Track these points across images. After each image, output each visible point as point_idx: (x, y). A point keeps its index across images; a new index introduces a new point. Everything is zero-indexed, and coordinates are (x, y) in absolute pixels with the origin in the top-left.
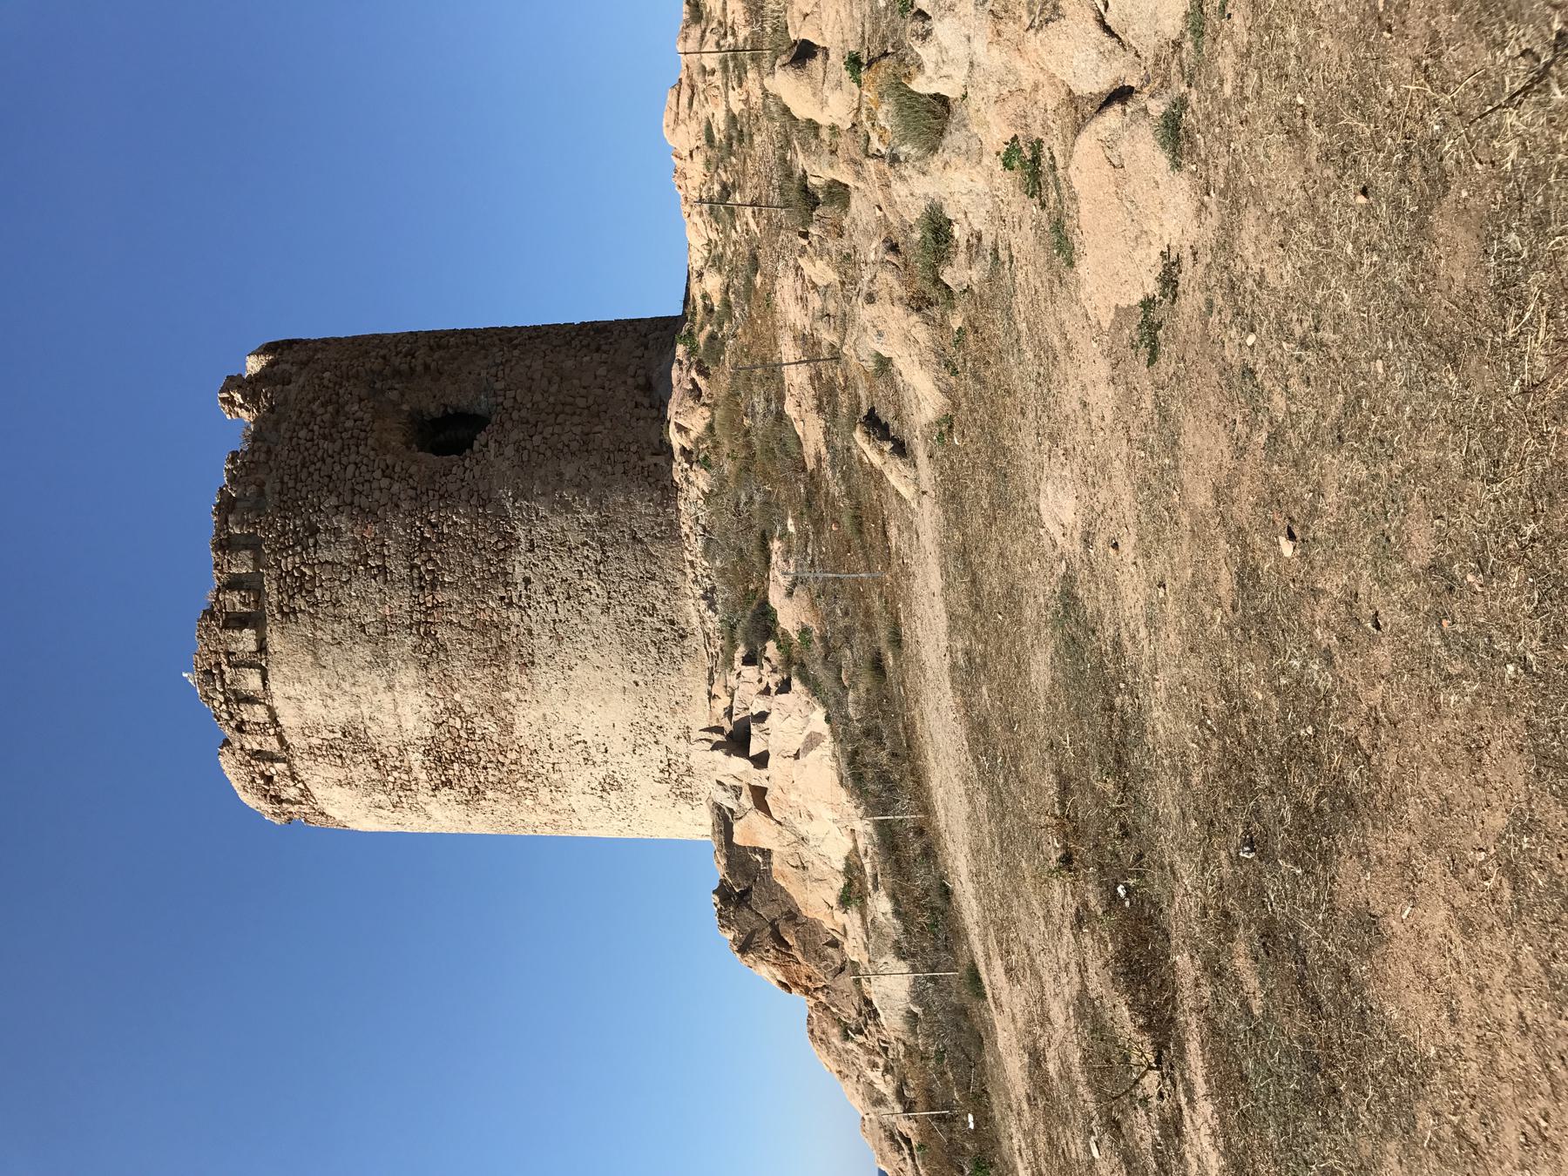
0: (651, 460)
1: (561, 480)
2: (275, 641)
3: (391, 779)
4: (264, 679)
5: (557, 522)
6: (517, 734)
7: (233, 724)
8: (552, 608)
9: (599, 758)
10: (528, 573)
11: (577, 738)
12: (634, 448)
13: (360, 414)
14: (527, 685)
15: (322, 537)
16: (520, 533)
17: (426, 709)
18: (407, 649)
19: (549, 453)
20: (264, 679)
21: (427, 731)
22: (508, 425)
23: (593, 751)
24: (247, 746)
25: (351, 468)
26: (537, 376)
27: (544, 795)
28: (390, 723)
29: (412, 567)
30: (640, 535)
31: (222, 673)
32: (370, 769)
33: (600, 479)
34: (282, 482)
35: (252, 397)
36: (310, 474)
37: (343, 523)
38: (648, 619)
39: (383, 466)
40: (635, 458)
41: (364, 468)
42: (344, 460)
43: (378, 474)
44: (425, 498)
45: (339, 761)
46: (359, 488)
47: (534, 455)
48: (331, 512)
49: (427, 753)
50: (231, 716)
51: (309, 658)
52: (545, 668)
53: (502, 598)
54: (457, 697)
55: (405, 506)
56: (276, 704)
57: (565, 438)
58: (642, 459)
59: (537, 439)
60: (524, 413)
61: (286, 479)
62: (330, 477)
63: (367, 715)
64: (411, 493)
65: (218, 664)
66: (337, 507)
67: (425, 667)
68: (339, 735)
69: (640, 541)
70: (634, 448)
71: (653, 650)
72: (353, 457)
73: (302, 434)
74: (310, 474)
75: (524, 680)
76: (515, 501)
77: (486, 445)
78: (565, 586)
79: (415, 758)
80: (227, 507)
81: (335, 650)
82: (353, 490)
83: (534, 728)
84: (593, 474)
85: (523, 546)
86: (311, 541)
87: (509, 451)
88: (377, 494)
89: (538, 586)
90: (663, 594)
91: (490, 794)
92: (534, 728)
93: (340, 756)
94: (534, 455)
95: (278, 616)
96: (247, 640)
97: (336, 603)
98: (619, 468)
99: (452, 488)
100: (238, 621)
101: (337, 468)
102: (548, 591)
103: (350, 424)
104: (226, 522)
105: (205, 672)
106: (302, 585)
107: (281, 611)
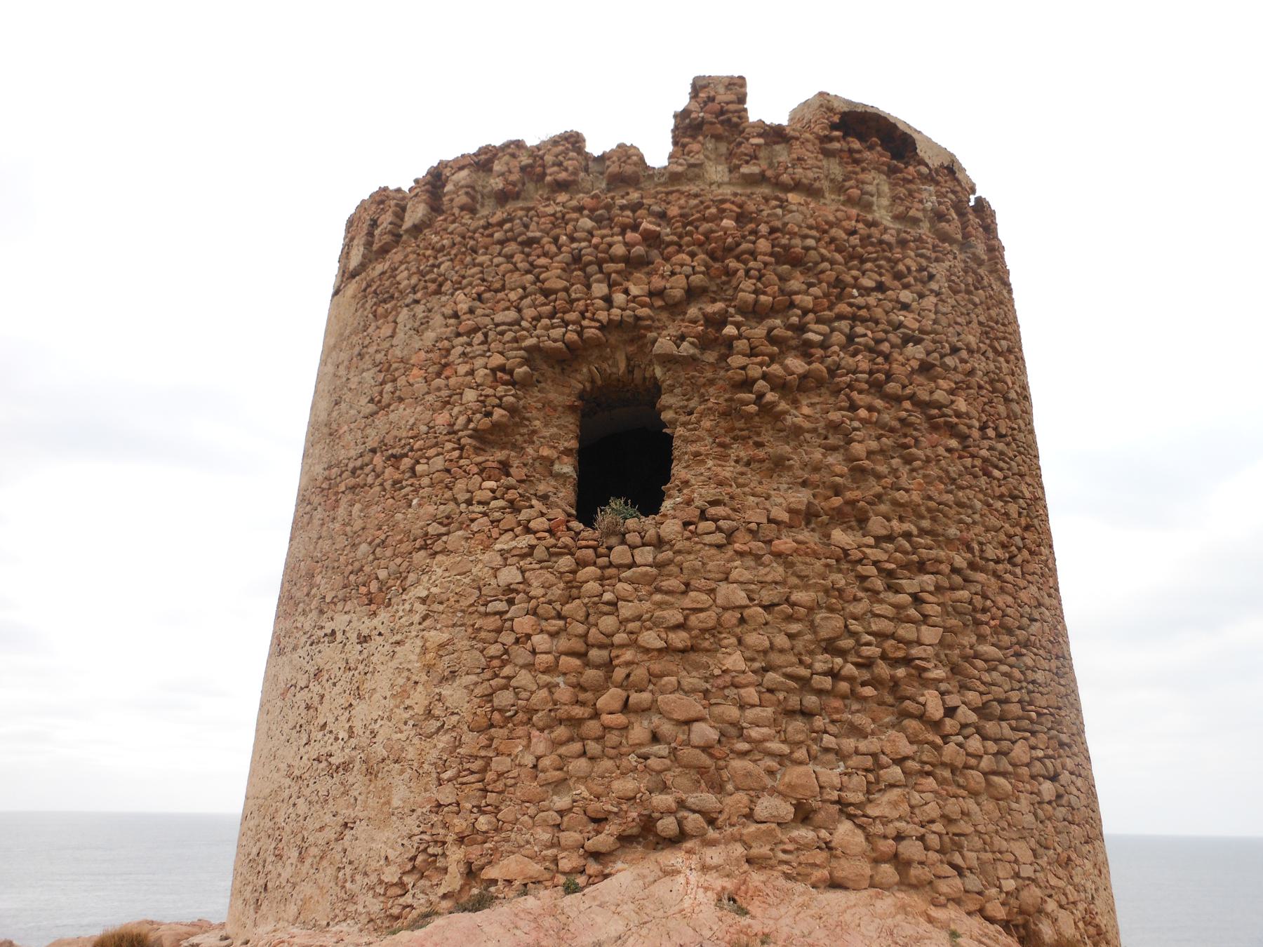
0: (455, 856)
1: (444, 679)
5: (382, 682)
10: (339, 636)
12: (483, 822)
13: (619, 298)
19: (494, 650)
22: (565, 562)
25: (512, 315)
26: (697, 598)
29: (374, 451)
33: (434, 754)
34: (501, 224)
35: (687, 128)
36: (509, 258)
39: (509, 364)
40: (459, 824)
41: (509, 336)
42: (527, 301)
43: (497, 360)
44: (449, 446)
46: (479, 337)
47: (493, 622)
48: (448, 311)
55: (442, 419)
57: (524, 678)
58: (461, 840)
59: (524, 624)
60: (593, 586)
61: (507, 226)
62: (503, 288)
64: (462, 420)
66: (456, 315)
69: (340, 838)
70: (483, 822)
72: (529, 313)
73: (586, 223)
74: (509, 258)
76: (423, 601)
77: (528, 530)
80: (484, 160)
82: (476, 329)
84: (443, 740)
87: (510, 575)
88: (463, 369)
94: (493, 622)
98: (446, 795)
101: (513, 296)
103: (600, 289)
104: (461, 168)
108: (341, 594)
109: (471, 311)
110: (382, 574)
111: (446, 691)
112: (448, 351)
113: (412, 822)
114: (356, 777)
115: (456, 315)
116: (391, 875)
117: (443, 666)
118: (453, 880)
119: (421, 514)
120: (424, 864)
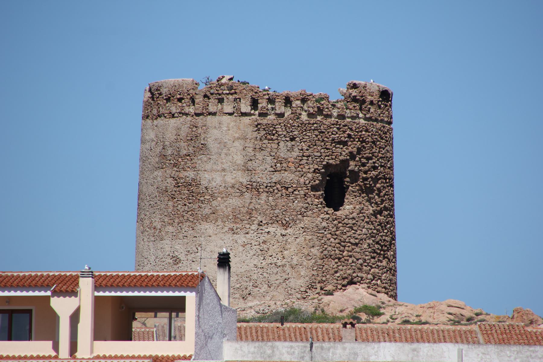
2: (246, 120)
3: (180, 160)
4: (230, 114)
6: (202, 222)
7: (208, 94)
8: (257, 243)
9: (190, 257)
11: (199, 248)
14: (224, 231)
15: (289, 144)
16: (289, 230)
17: (214, 184)
18: (241, 180)
20: (230, 114)
21: (204, 183)
23: (193, 255)
24: (197, 97)
27: (170, 229)
28: (208, 167)
30: (287, 282)
31: (232, 94)
32: (185, 152)
37: (296, 153)
38: (251, 284)
40: (319, 279)
45: (189, 138)
49: (193, 180)
50: (212, 94)
51: (237, 135)
52: (231, 238)
53: (261, 222)
54: (219, 199)
55: (302, 180)
56: (217, 117)
63: (211, 157)
65: (236, 93)
67: (233, 187)
68: (202, 142)
71: (238, 286)
75: (226, 229)
78: (266, 249)
79: (191, 174)
81: (241, 148)
83: (205, 231)
85: (284, 232)
86: (288, 139)
87: (324, 224)
89: (267, 237)
90: (261, 291)
91: (170, 203)
92: (205, 231)
93: (191, 139)
95: (256, 123)
96: (245, 107)
97: (261, 149)
98: (315, 273)
99: (309, 200)
100: (254, 104)
102: (264, 242)
105: (232, 86)
106: (269, 133)
107: (259, 124)
108: (270, 222)
109: (307, 150)
110: (287, 219)
111: (312, 250)
112: (301, 160)
113: (307, 278)
114: (288, 269)
115: (302, 150)
116: (303, 289)
117: (311, 244)
118: (318, 290)
119: (298, 205)
120: (311, 287)
